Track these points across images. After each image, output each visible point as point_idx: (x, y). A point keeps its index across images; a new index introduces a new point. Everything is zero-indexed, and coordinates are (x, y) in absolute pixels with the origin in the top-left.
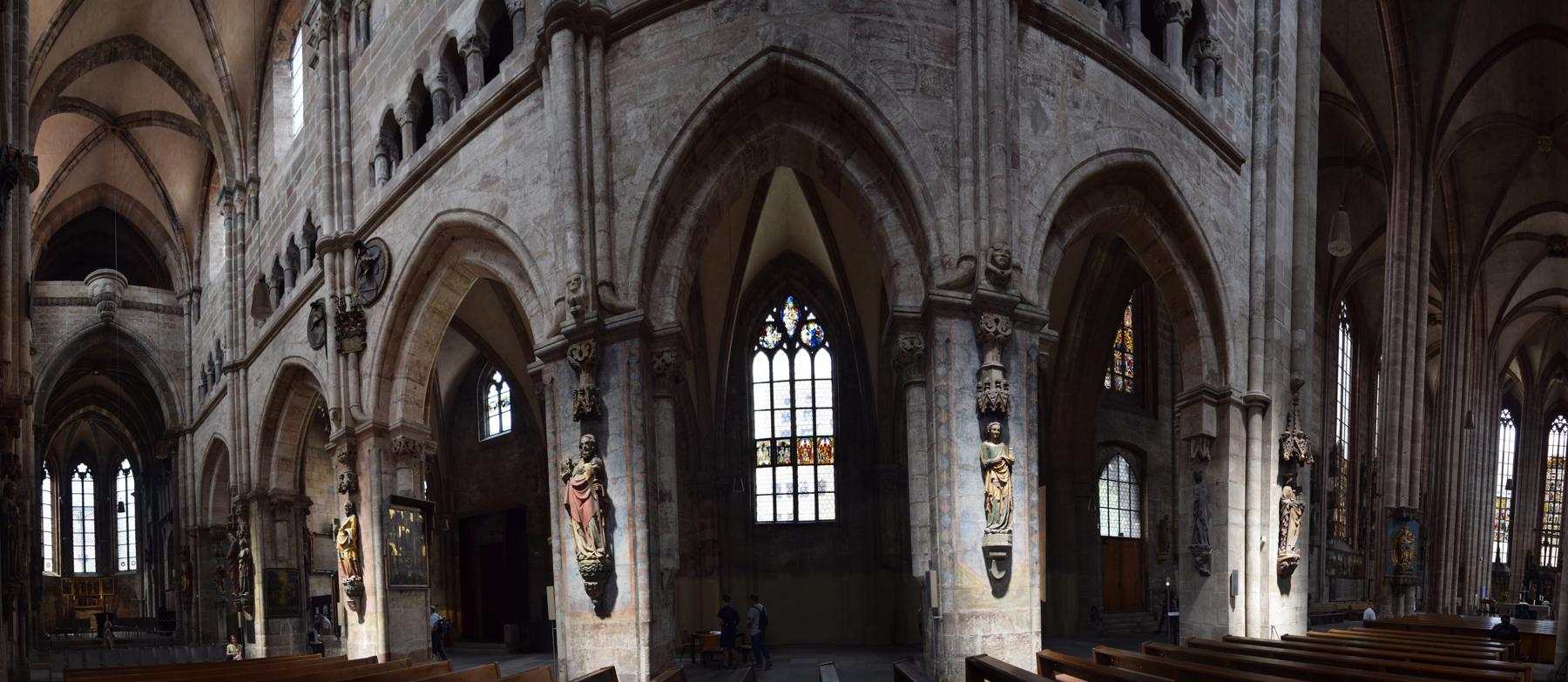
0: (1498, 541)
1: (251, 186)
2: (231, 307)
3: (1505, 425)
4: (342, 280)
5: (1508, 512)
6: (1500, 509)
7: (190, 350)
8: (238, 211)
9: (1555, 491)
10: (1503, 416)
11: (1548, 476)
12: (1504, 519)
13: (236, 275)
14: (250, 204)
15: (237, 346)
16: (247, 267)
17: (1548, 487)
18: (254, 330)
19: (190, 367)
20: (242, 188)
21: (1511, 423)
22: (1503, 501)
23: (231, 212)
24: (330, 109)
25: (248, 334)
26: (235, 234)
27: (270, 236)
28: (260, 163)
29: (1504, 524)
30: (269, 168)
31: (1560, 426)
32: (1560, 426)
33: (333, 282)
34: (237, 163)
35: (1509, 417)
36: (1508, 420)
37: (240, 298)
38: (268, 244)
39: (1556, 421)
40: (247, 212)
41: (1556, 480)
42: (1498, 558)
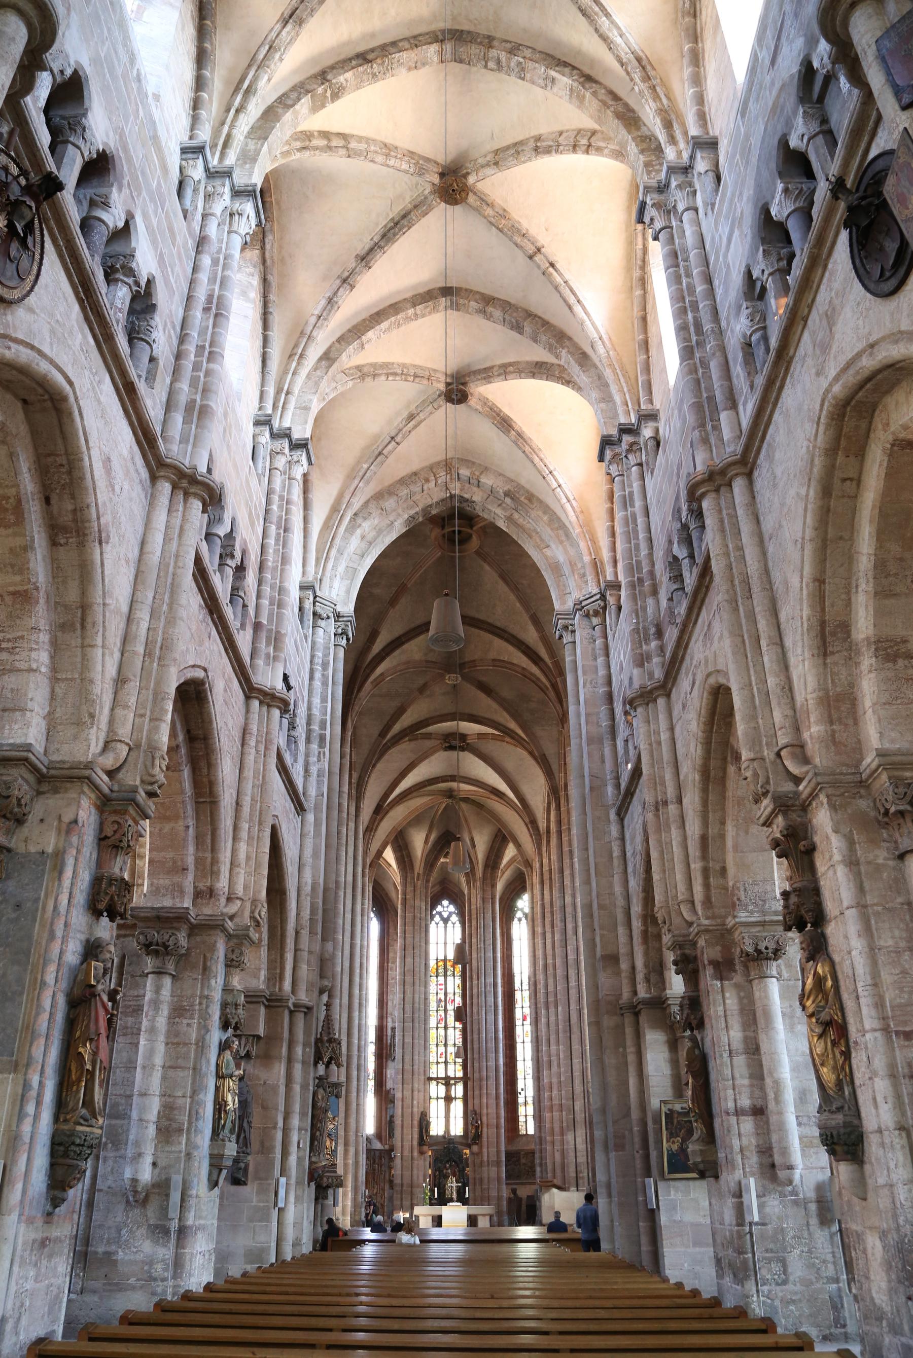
9: (446, 1010)
11: (433, 988)
17: (433, 1005)
31: (445, 915)
32: (445, 915)
39: (439, 908)
41: (446, 994)
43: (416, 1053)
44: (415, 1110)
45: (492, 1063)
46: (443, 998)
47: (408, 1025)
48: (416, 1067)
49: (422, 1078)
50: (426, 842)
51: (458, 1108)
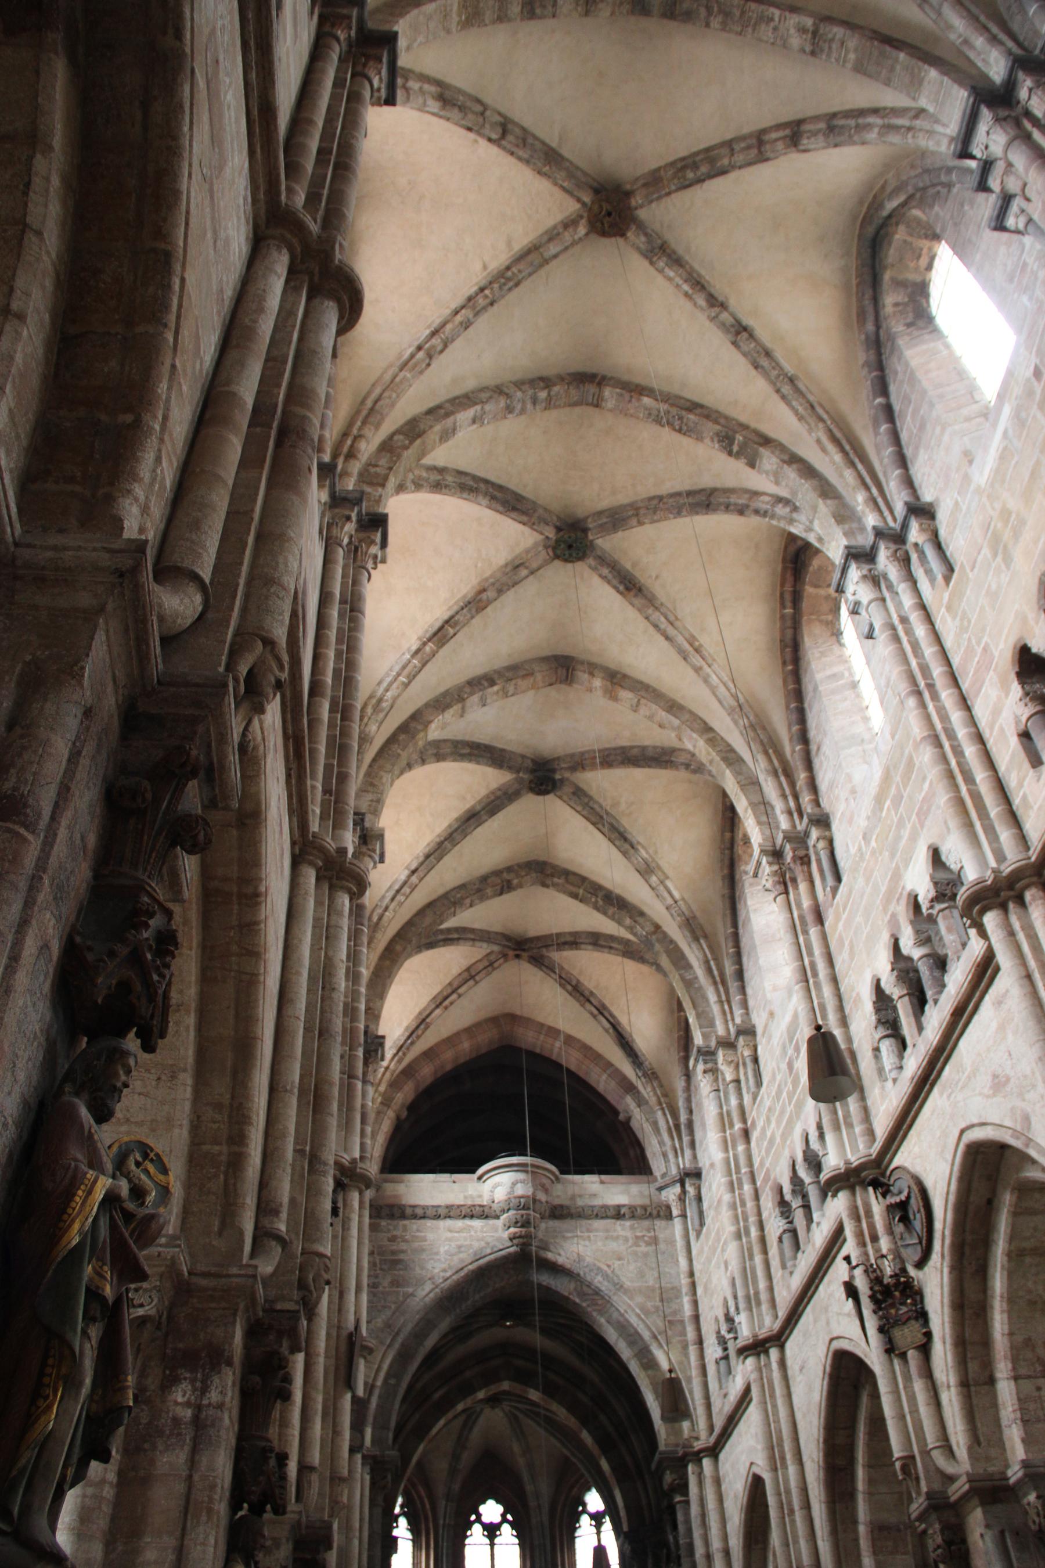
1: (741, 1040)
2: (738, 1236)
4: (872, 1226)
7: (693, 1285)
8: (729, 1077)
13: (739, 1180)
14: (744, 1064)
15: (759, 1303)
16: (756, 1165)
18: (783, 1276)
19: (696, 1318)
20: (729, 1045)
23: (716, 1080)
24: (807, 981)
25: (775, 1281)
26: (729, 1113)
27: (778, 1127)
28: (751, 1003)
30: (764, 1015)
33: (859, 1235)
34: (716, 1009)
37: (752, 1219)
38: (778, 1140)
40: (742, 1078)
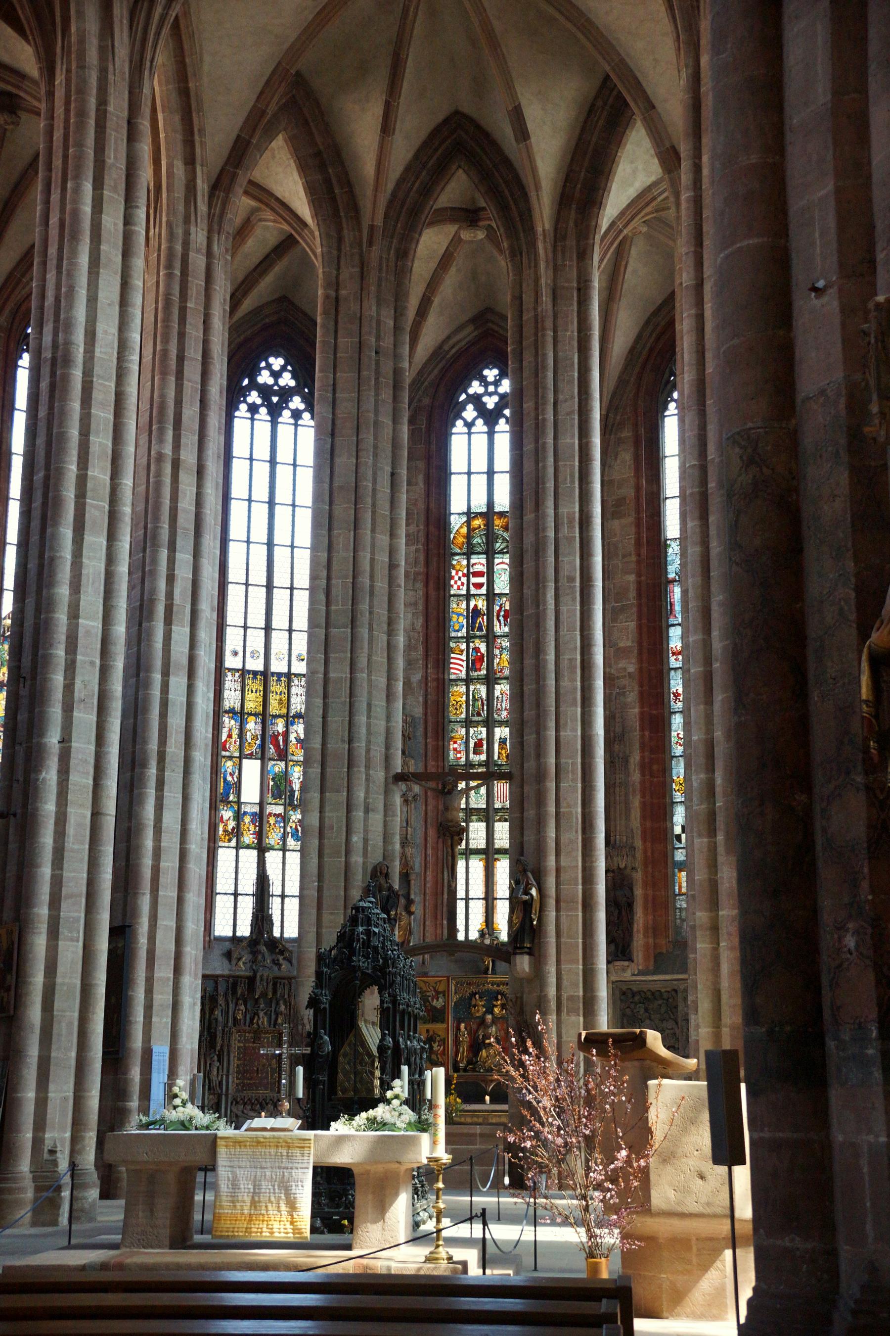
0: (262, 849)
3: (275, 412)
5: (299, 729)
6: (264, 717)
9: (490, 638)
10: (264, 378)
11: (457, 585)
12: (283, 755)
17: (459, 624)
21: (297, 403)
22: (276, 687)
29: (285, 777)
31: (491, 402)
32: (491, 402)
35: (287, 380)
36: (286, 394)
39: (476, 387)
41: (491, 597)
42: (261, 918)
43: (361, 705)
44: (357, 859)
45: (573, 733)
46: (482, 604)
47: (341, 632)
48: (361, 745)
49: (379, 775)
50: (387, 128)
51: (503, 868)
